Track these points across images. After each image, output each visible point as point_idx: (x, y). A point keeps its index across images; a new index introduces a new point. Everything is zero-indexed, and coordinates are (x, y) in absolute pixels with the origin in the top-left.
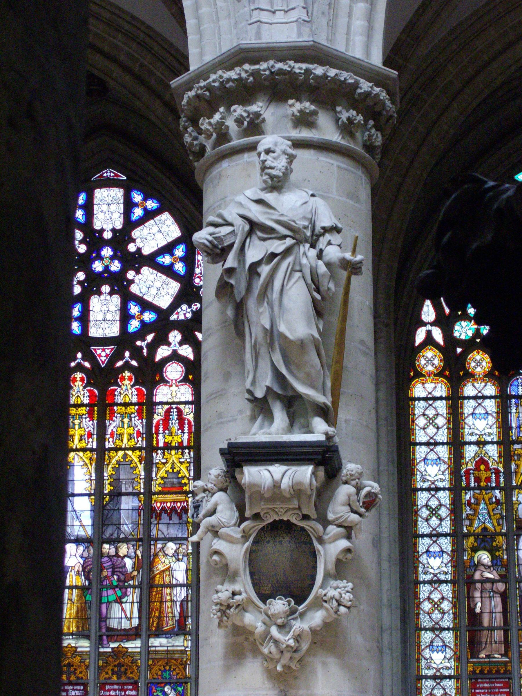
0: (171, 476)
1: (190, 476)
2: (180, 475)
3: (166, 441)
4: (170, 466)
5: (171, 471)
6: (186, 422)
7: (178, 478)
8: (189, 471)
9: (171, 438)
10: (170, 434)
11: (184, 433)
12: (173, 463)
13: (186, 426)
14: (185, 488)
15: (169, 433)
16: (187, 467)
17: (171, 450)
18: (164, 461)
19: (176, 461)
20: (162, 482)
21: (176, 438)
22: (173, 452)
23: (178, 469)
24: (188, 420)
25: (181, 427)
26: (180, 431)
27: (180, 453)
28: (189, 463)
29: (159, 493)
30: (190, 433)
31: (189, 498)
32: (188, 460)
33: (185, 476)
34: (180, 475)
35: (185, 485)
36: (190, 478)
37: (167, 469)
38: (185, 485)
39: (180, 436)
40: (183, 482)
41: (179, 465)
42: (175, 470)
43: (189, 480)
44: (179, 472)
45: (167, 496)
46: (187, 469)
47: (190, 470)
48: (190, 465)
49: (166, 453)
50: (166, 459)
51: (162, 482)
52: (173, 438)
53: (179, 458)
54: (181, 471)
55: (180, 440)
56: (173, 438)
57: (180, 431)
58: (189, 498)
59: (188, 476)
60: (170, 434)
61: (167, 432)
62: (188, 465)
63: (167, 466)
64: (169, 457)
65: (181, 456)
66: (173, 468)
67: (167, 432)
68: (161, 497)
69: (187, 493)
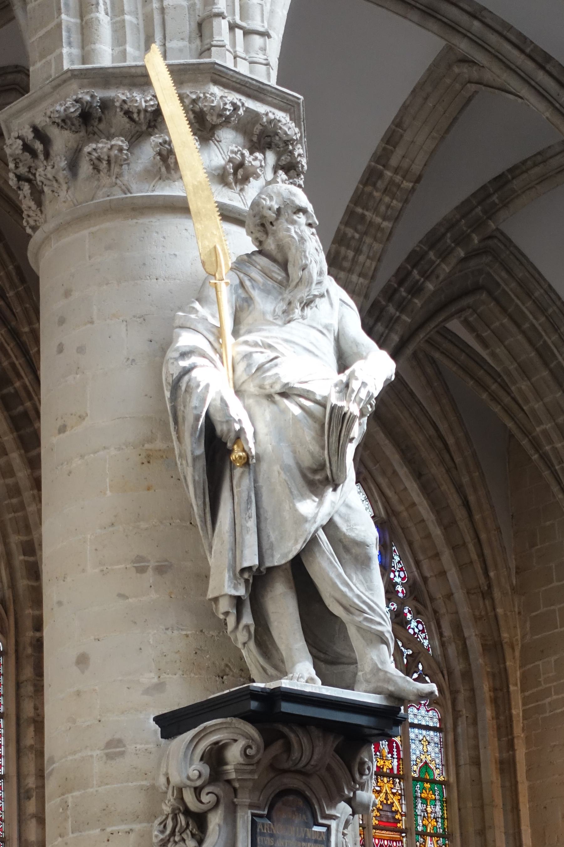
0: (386, 808)
1: (402, 811)
2: (393, 809)
3: (379, 765)
4: (384, 796)
5: (385, 802)
6: (395, 745)
7: (392, 812)
8: (401, 805)
9: (382, 763)
10: (382, 757)
11: (394, 758)
12: (386, 793)
13: (395, 750)
14: (399, 825)
15: (380, 756)
16: (399, 800)
17: (384, 777)
18: (378, 789)
19: (389, 792)
20: (378, 814)
21: (387, 763)
22: (385, 780)
23: (392, 801)
24: (396, 743)
25: (391, 752)
26: (390, 755)
27: (391, 782)
28: (401, 795)
29: (375, 827)
30: (399, 759)
31: (403, 837)
32: (400, 792)
33: (398, 811)
34: (393, 809)
35: (399, 821)
36: (402, 813)
37: (382, 800)
38: (399, 821)
39: (390, 762)
40: (397, 817)
41: (392, 796)
42: (389, 802)
43: (402, 815)
44: (392, 804)
45: (383, 832)
46: (399, 802)
47: (402, 804)
48: (401, 798)
49: (379, 780)
50: (380, 787)
51: (378, 814)
52: (384, 762)
53: (392, 788)
54: (394, 804)
55: (390, 767)
56: (384, 762)
57: (390, 755)
58: (403, 837)
59: (400, 811)
60: (382, 757)
61: (378, 753)
62: (399, 797)
63: (381, 795)
64: (382, 784)
65: (393, 786)
66: (387, 799)
67: (378, 753)
68: (378, 833)
69: (401, 831)
